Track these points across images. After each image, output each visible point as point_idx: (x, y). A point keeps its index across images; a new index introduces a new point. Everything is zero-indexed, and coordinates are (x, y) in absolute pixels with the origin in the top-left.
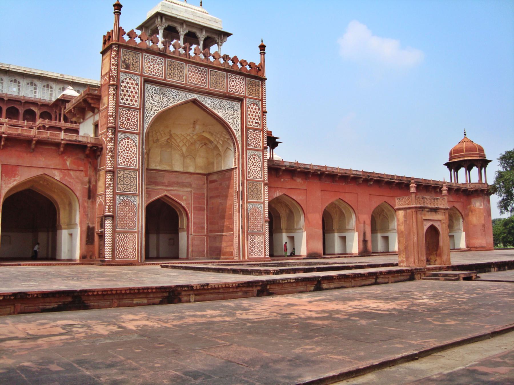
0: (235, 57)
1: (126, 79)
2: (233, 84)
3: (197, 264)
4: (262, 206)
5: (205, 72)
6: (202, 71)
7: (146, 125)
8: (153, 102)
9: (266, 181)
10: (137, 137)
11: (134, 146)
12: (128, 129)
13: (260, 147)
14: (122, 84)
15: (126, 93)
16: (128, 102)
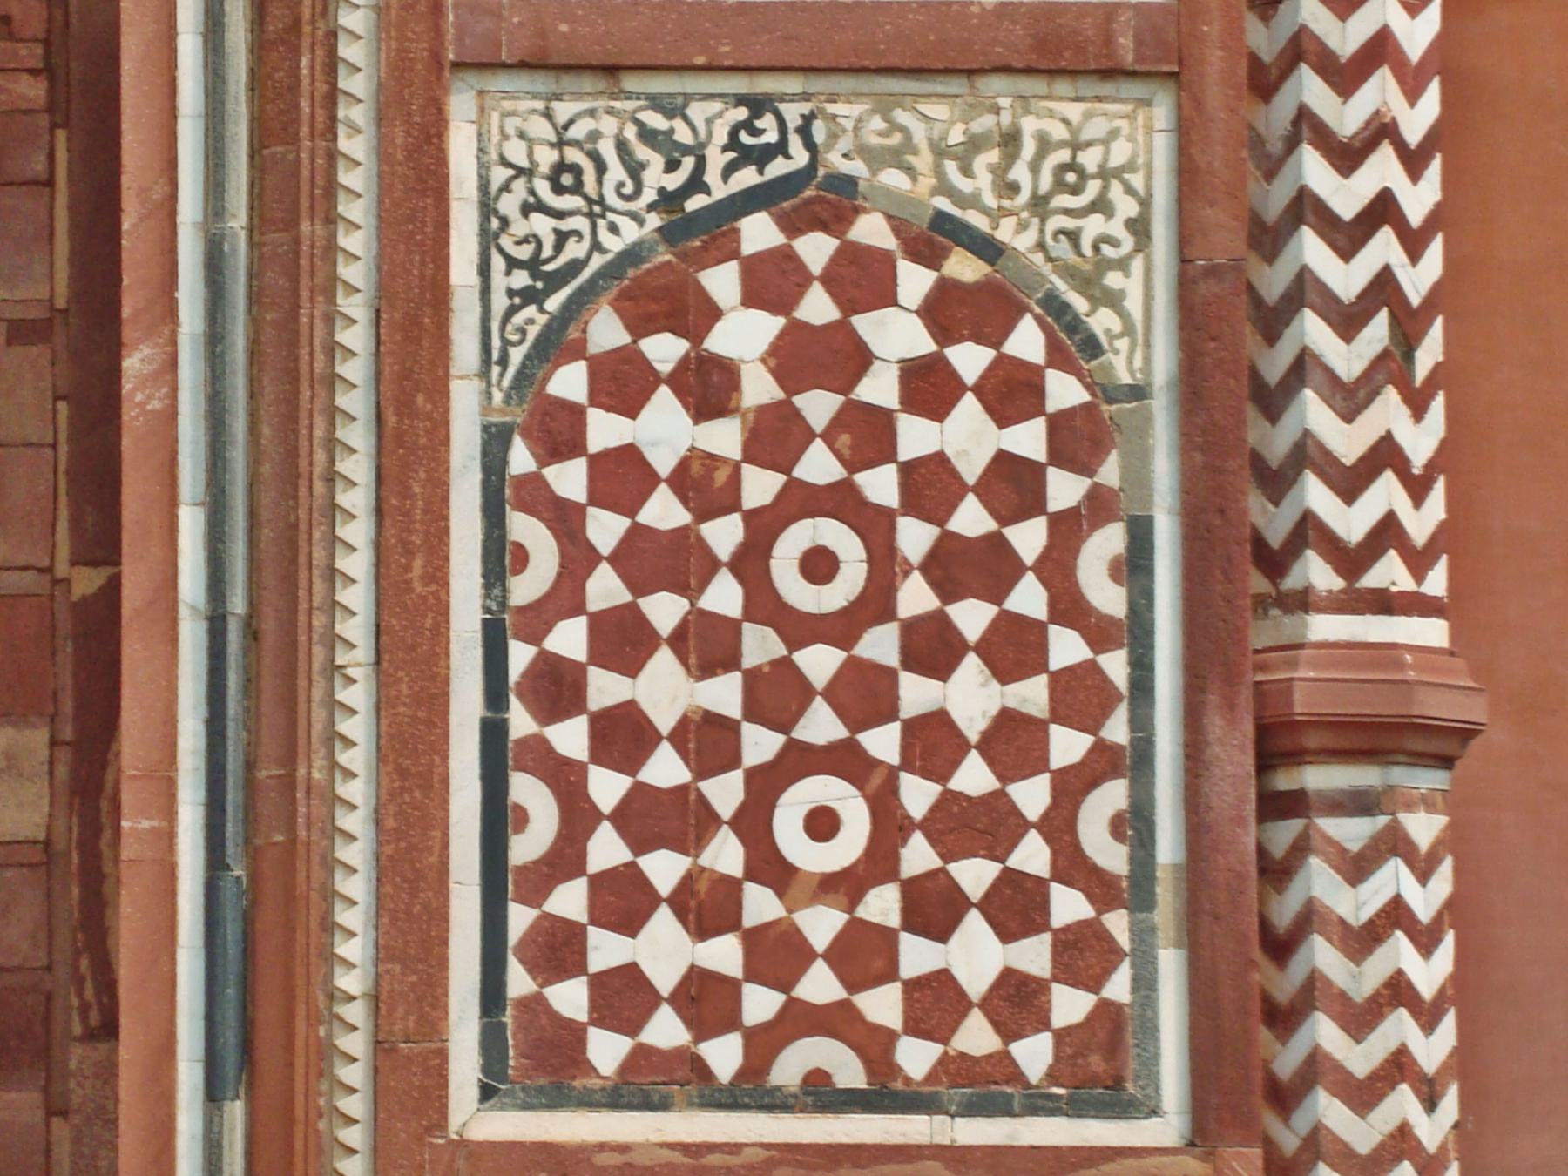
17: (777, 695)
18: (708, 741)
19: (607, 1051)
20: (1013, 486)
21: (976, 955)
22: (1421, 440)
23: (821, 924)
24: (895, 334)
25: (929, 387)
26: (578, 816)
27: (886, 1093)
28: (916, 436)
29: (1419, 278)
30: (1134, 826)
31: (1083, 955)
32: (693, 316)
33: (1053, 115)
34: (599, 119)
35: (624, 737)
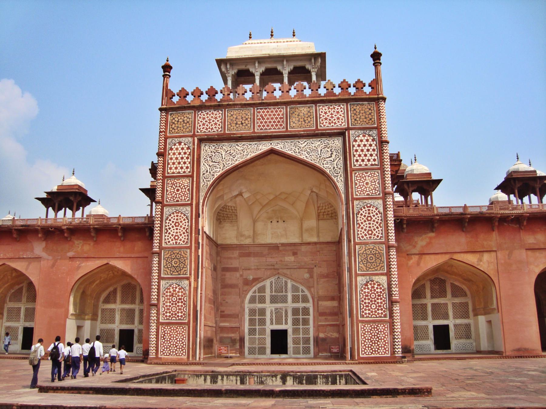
0: (359, 81)
1: (175, 145)
2: (326, 116)
3: (248, 366)
4: (385, 278)
5: (280, 111)
6: (276, 112)
7: (202, 194)
8: (211, 164)
9: (393, 242)
10: (189, 208)
11: (184, 220)
12: (177, 201)
13: (379, 194)
14: (170, 152)
15: (175, 161)
16: (178, 171)
17: (371, 301)
18: (369, 303)
19: (365, 316)
20: (381, 292)
21: (380, 311)
22: (397, 290)
23: (374, 310)
24: (376, 286)
25: (377, 288)
26: (364, 306)
27: (377, 317)
28: (377, 290)
29: (397, 283)
30: (386, 306)
31: (384, 311)
32: (367, 286)
33: (382, 277)
34: (363, 278)
35: (365, 303)
